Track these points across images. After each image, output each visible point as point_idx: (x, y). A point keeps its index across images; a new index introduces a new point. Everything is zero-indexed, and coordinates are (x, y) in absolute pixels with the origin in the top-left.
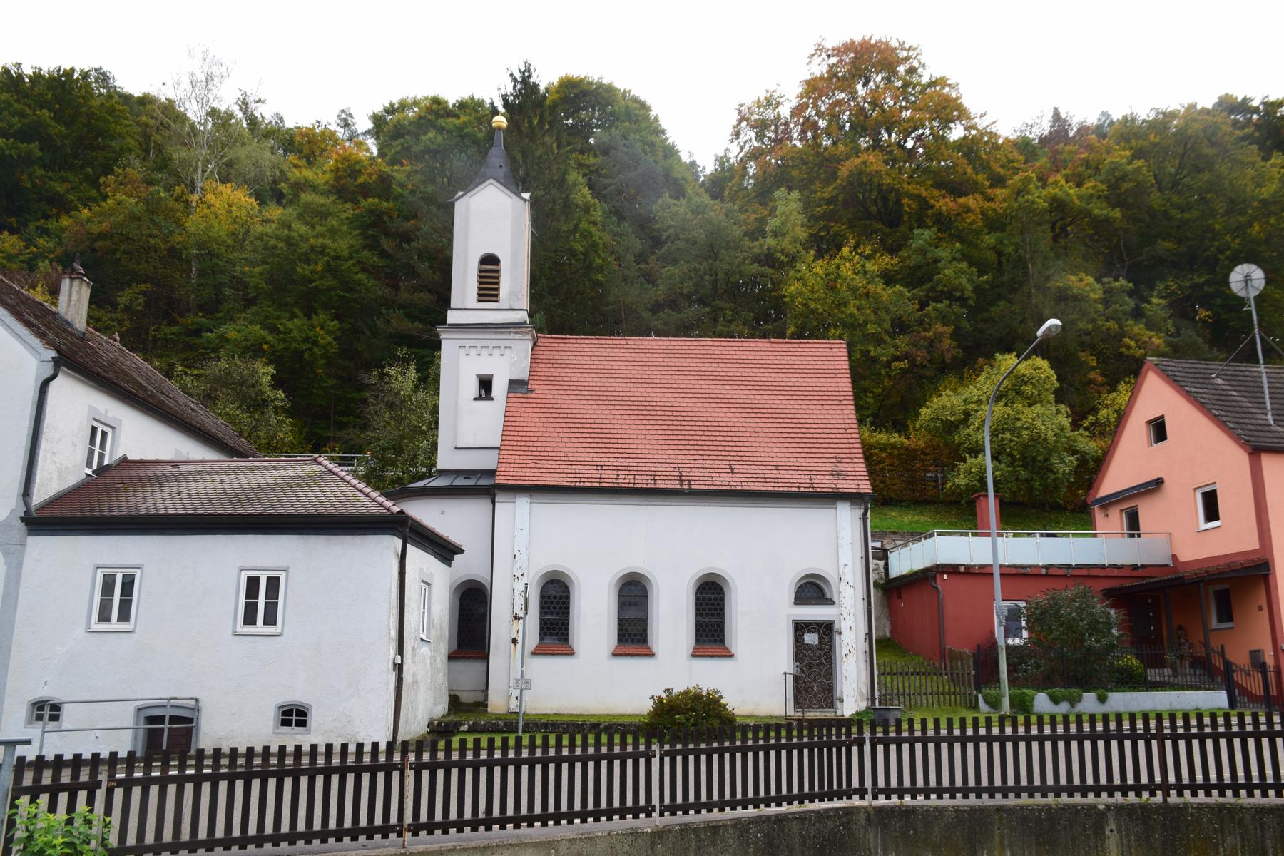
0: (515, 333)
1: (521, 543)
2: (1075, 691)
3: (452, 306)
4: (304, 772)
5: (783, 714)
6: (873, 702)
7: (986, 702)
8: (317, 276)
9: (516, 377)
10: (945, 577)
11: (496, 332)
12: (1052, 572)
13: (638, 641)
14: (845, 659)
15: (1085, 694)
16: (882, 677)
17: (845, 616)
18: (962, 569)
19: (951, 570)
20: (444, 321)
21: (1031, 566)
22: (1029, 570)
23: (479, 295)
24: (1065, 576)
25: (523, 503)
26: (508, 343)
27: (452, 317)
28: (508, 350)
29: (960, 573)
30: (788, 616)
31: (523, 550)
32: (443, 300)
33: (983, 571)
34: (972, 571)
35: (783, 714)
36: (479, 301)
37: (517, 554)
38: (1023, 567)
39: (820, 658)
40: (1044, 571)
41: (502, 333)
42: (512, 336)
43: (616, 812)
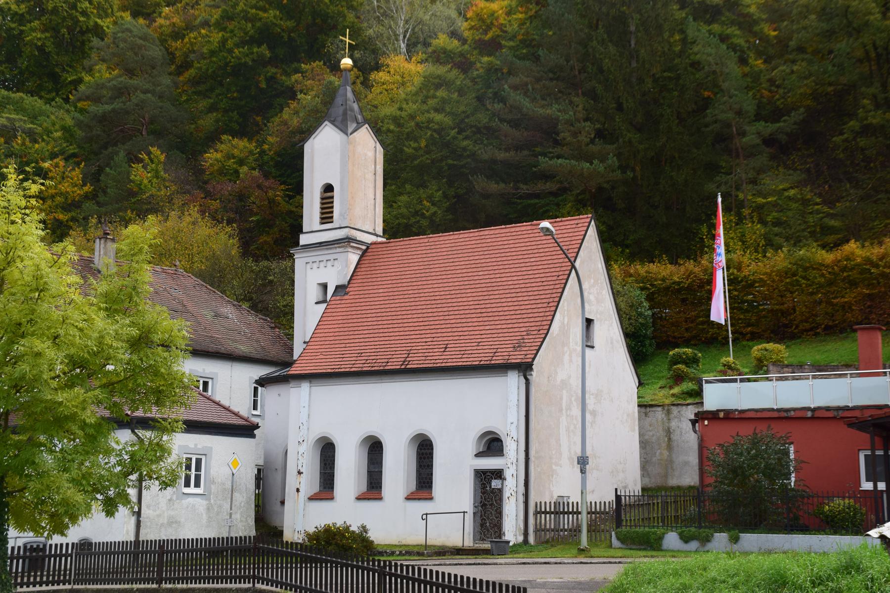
0: (339, 247)
1: (304, 417)
2: (704, 532)
3: (304, 231)
4: (15, 558)
5: (424, 543)
6: (526, 534)
7: (618, 538)
8: (421, 152)
9: (340, 283)
10: (706, 422)
11: (327, 249)
12: (817, 414)
13: (426, 487)
14: (507, 501)
15: (717, 535)
16: (589, 516)
17: (509, 465)
18: (722, 415)
19: (710, 416)
20: (297, 243)
21: (795, 410)
22: (792, 413)
23: (322, 219)
24: (834, 418)
25: (305, 386)
26: (335, 256)
27: (304, 239)
28: (336, 261)
29: (719, 419)
30: (471, 466)
31: (305, 423)
32: (297, 229)
33: (743, 416)
34: (731, 416)
35: (424, 543)
36: (322, 223)
37: (301, 425)
38: (787, 410)
39: (492, 499)
40: (809, 414)
41: (331, 248)
42: (338, 250)
43: (61, 581)
